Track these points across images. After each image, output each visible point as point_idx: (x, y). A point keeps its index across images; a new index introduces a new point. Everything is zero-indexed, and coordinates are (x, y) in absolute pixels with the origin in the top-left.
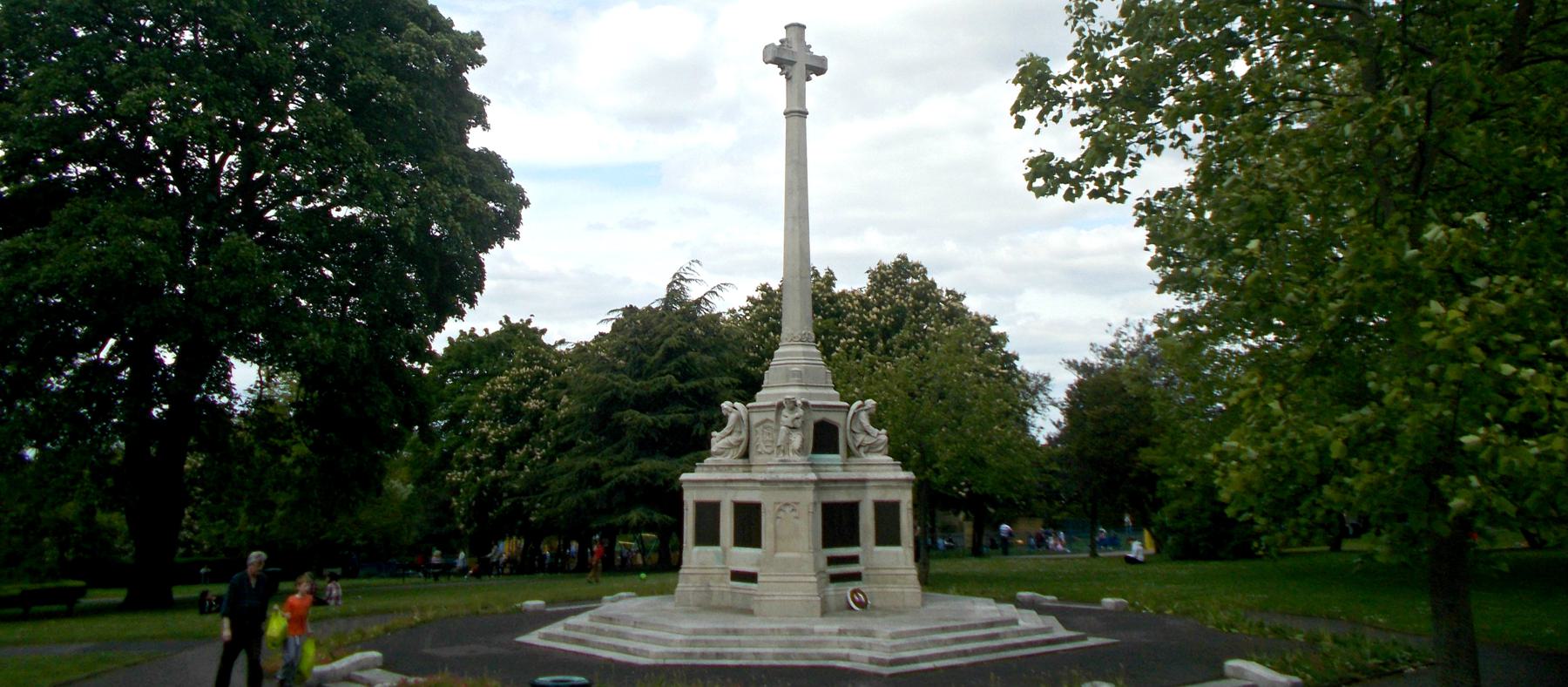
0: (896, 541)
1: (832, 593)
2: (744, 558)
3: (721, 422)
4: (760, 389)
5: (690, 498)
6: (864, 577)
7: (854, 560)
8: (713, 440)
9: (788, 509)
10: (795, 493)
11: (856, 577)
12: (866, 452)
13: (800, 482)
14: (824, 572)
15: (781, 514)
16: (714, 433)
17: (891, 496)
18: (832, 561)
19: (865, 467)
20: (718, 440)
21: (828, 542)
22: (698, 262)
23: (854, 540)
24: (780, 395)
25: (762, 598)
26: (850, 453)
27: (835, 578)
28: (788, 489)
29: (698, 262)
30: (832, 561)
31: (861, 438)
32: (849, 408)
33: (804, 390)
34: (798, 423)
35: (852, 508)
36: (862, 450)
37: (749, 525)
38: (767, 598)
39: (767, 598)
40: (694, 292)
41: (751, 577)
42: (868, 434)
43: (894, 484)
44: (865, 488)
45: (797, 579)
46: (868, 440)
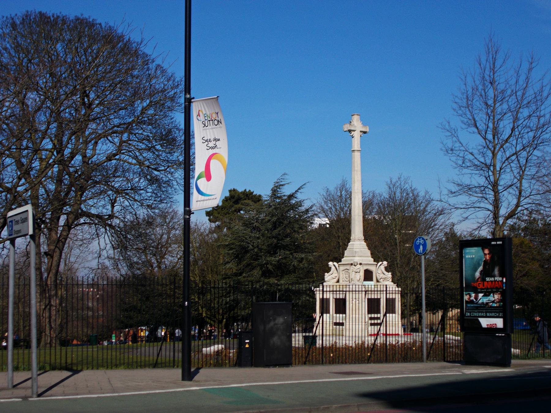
2: (339, 318)
3: (328, 270)
4: (343, 257)
5: (318, 296)
8: (326, 276)
16: (326, 274)
18: (371, 319)
20: (327, 276)
21: (369, 312)
24: (351, 260)
26: (378, 281)
27: (371, 324)
30: (371, 319)
31: (382, 275)
32: (377, 265)
34: (358, 270)
35: (378, 300)
37: (341, 306)
40: (286, 191)
41: (342, 324)
46: (384, 276)
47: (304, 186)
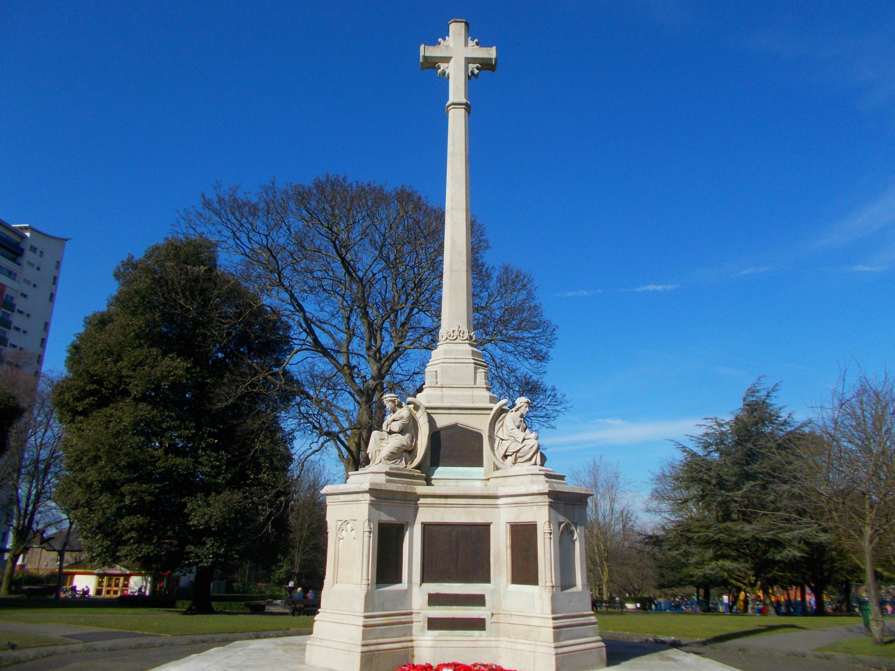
0: (534, 581)
1: (430, 643)
7: (478, 600)
9: (349, 526)
11: (478, 624)
12: (515, 463)
17: (525, 516)
22: (763, 376)
29: (763, 376)
30: (435, 600)
33: (438, 392)
36: (510, 459)
44: (495, 506)
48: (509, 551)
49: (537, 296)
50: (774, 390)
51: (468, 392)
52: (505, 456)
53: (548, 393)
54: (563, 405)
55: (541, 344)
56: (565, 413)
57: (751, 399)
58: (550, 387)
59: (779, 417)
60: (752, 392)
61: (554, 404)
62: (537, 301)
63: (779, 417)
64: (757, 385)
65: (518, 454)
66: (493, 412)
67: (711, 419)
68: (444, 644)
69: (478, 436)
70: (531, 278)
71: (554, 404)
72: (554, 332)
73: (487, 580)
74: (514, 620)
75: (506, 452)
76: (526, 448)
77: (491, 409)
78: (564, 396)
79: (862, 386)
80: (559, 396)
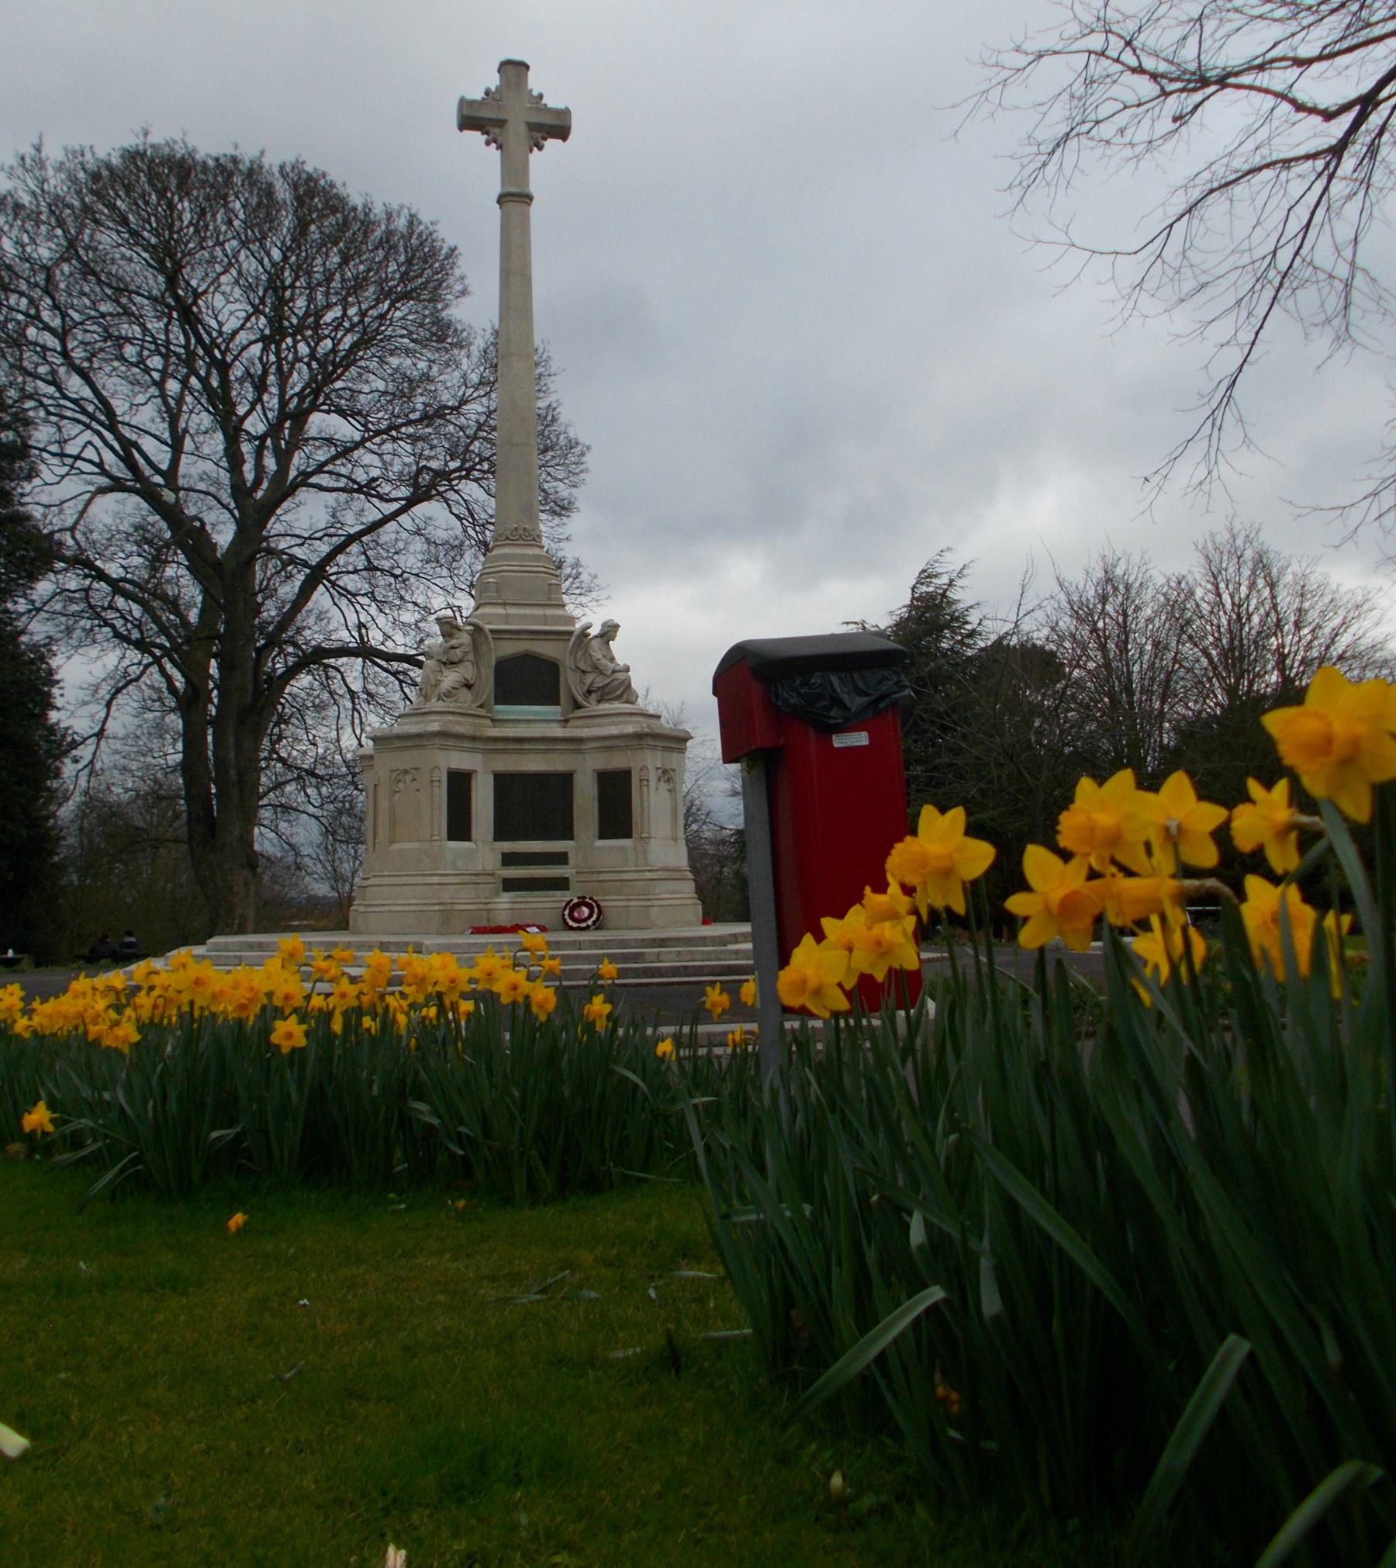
1: (506, 906)
6: (573, 884)
7: (561, 858)
9: (408, 778)
10: (416, 753)
12: (599, 702)
13: (419, 736)
14: (493, 874)
15: (401, 785)
18: (509, 859)
19: (587, 721)
22: (949, 549)
23: (566, 831)
25: (370, 909)
27: (510, 885)
28: (407, 748)
29: (949, 549)
30: (509, 859)
38: (376, 909)
39: (376, 909)
42: (601, 673)
43: (620, 743)
44: (580, 751)
45: (413, 880)
46: (600, 682)
47: (965, 572)
48: (596, 803)
49: (552, 387)
50: (960, 574)
51: (539, 611)
52: (589, 692)
53: (567, 571)
54: (594, 595)
55: (556, 479)
56: (595, 609)
57: (924, 589)
58: (570, 560)
59: (967, 623)
60: (926, 576)
61: (578, 592)
62: (552, 398)
63: (967, 623)
64: (936, 565)
65: (606, 690)
66: (573, 639)
67: (856, 623)
68: (523, 906)
69: (551, 668)
70: (544, 357)
71: (578, 592)
72: (584, 459)
73: (571, 838)
74: (602, 877)
75: (590, 685)
76: (616, 683)
77: (570, 633)
78: (596, 577)
79: (1106, 572)
80: (585, 577)
